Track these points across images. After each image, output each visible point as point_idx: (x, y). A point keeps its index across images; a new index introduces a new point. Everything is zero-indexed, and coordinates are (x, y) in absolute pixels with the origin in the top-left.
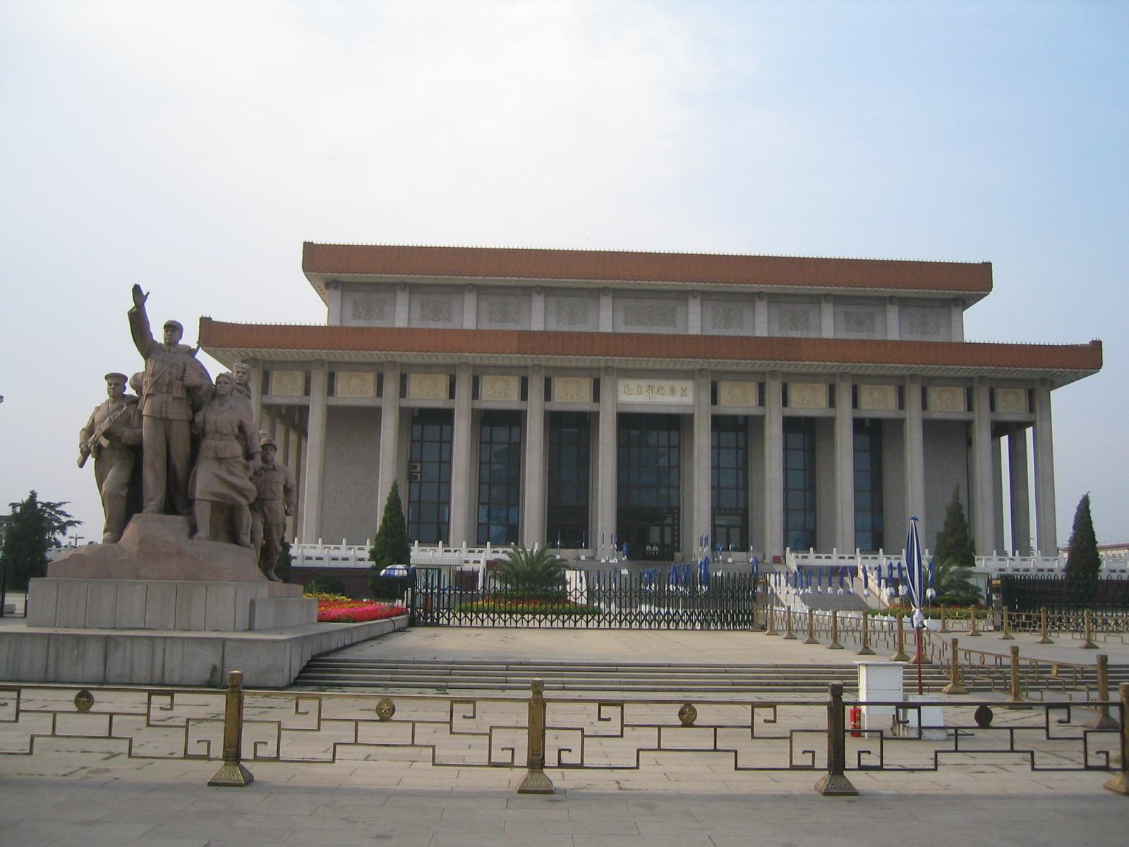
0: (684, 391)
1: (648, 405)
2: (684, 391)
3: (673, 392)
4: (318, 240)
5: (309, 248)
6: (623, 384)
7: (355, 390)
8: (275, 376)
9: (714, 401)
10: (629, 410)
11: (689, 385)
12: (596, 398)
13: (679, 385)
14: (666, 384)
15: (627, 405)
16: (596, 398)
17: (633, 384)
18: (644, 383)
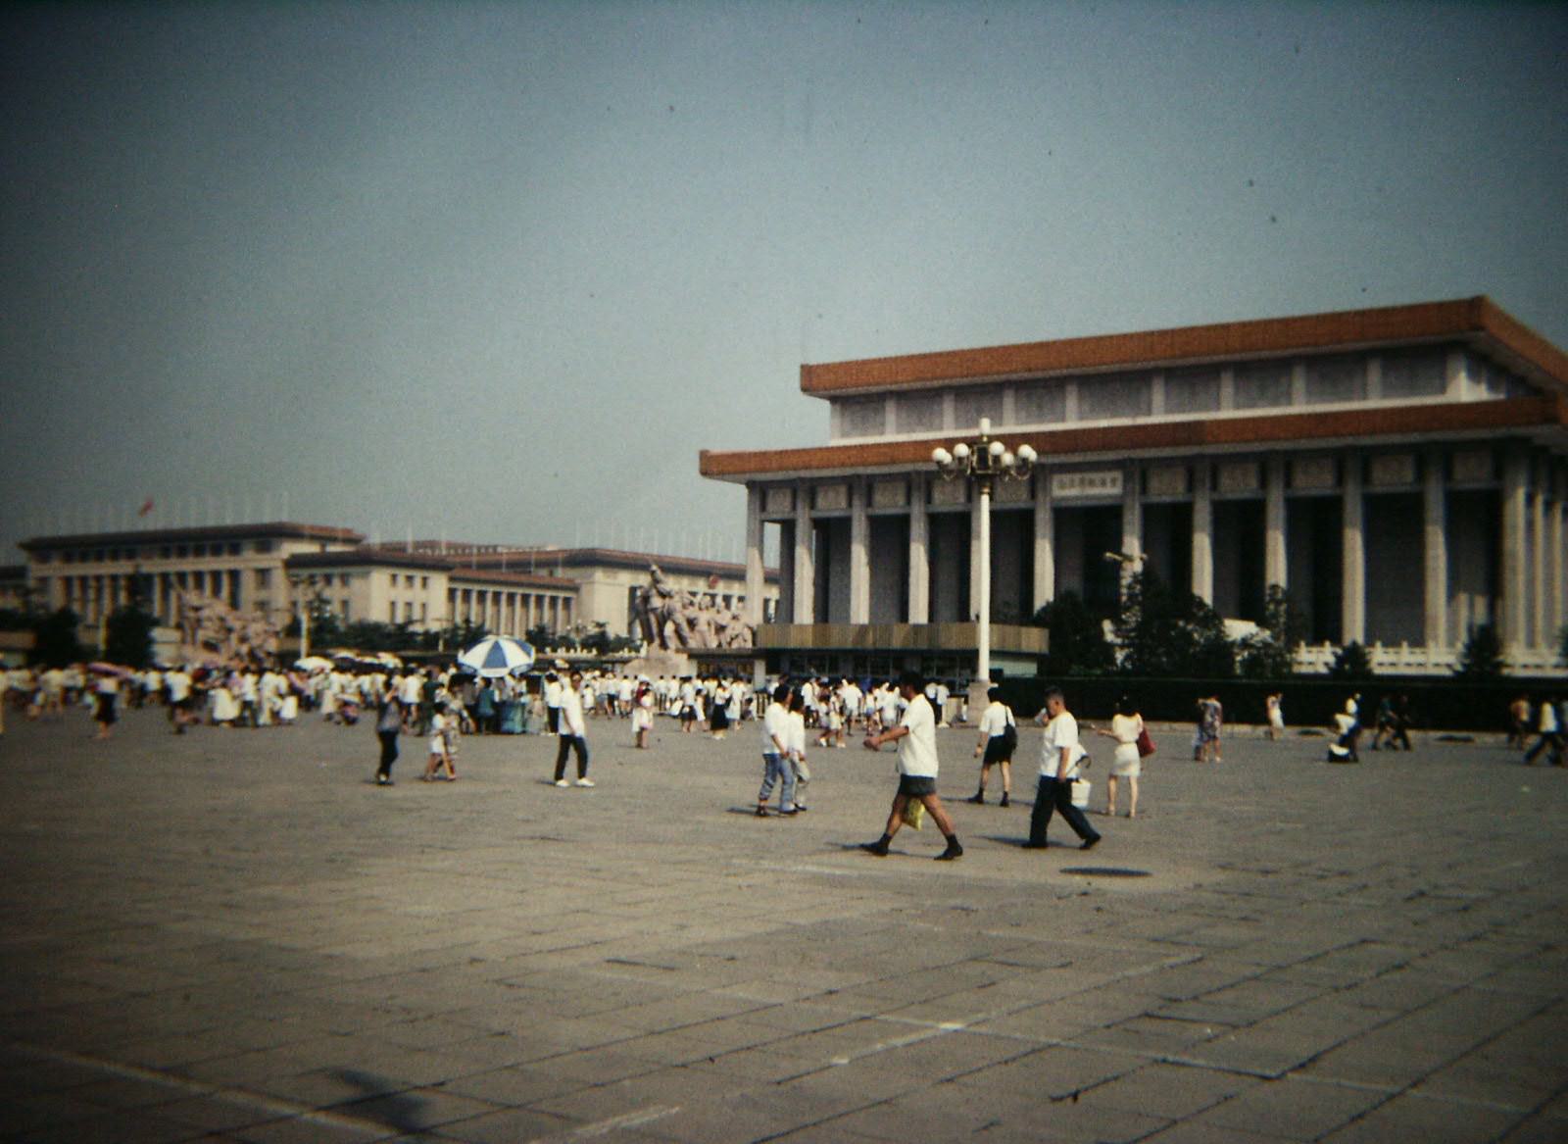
0: (1114, 481)
1: (1077, 498)
2: (1114, 481)
3: (1103, 483)
4: (813, 361)
5: (807, 371)
6: (1056, 479)
7: (831, 504)
8: (771, 493)
9: (1144, 490)
10: (1064, 504)
11: (1118, 475)
12: (1033, 495)
13: (1109, 476)
14: (1096, 476)
15: (1063, 499)
16: (1033, 495)
17: (1066, 478)
18: (1077, 477)
